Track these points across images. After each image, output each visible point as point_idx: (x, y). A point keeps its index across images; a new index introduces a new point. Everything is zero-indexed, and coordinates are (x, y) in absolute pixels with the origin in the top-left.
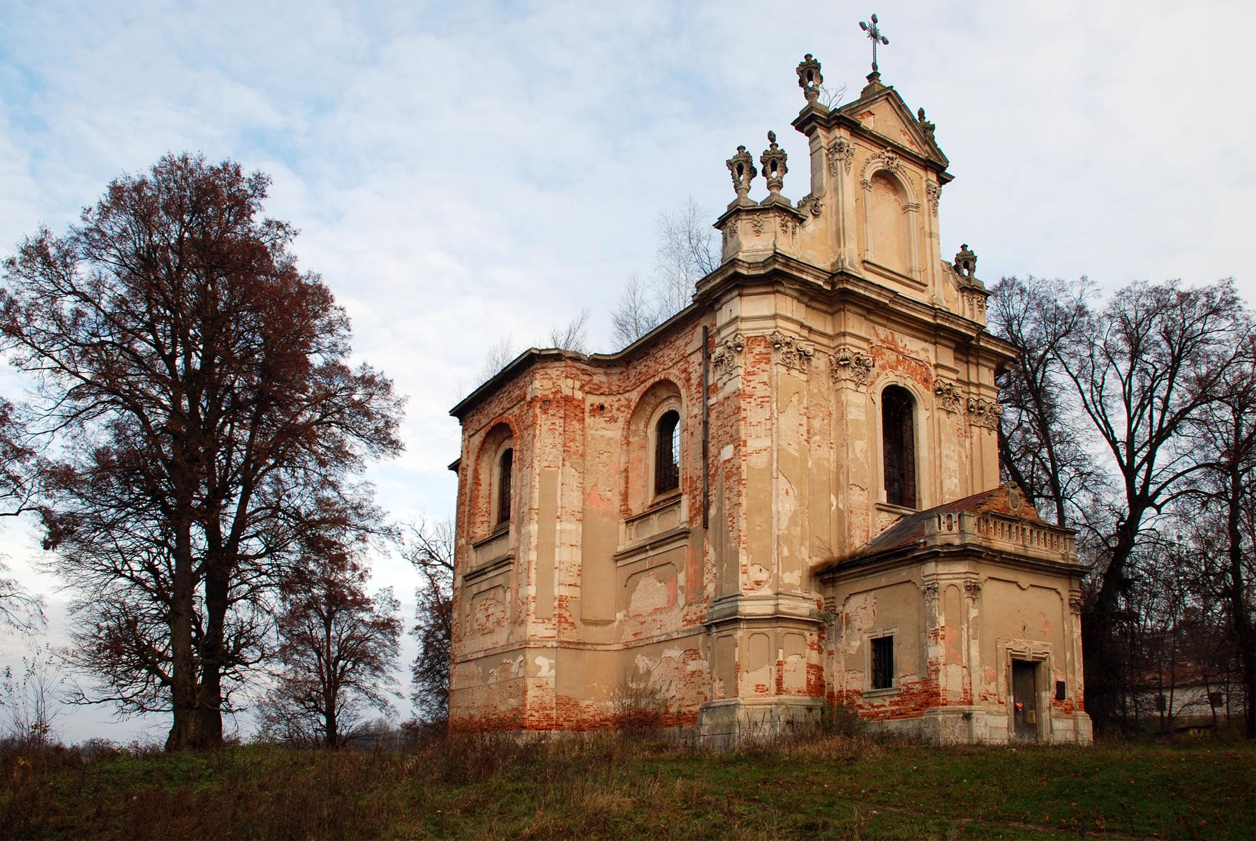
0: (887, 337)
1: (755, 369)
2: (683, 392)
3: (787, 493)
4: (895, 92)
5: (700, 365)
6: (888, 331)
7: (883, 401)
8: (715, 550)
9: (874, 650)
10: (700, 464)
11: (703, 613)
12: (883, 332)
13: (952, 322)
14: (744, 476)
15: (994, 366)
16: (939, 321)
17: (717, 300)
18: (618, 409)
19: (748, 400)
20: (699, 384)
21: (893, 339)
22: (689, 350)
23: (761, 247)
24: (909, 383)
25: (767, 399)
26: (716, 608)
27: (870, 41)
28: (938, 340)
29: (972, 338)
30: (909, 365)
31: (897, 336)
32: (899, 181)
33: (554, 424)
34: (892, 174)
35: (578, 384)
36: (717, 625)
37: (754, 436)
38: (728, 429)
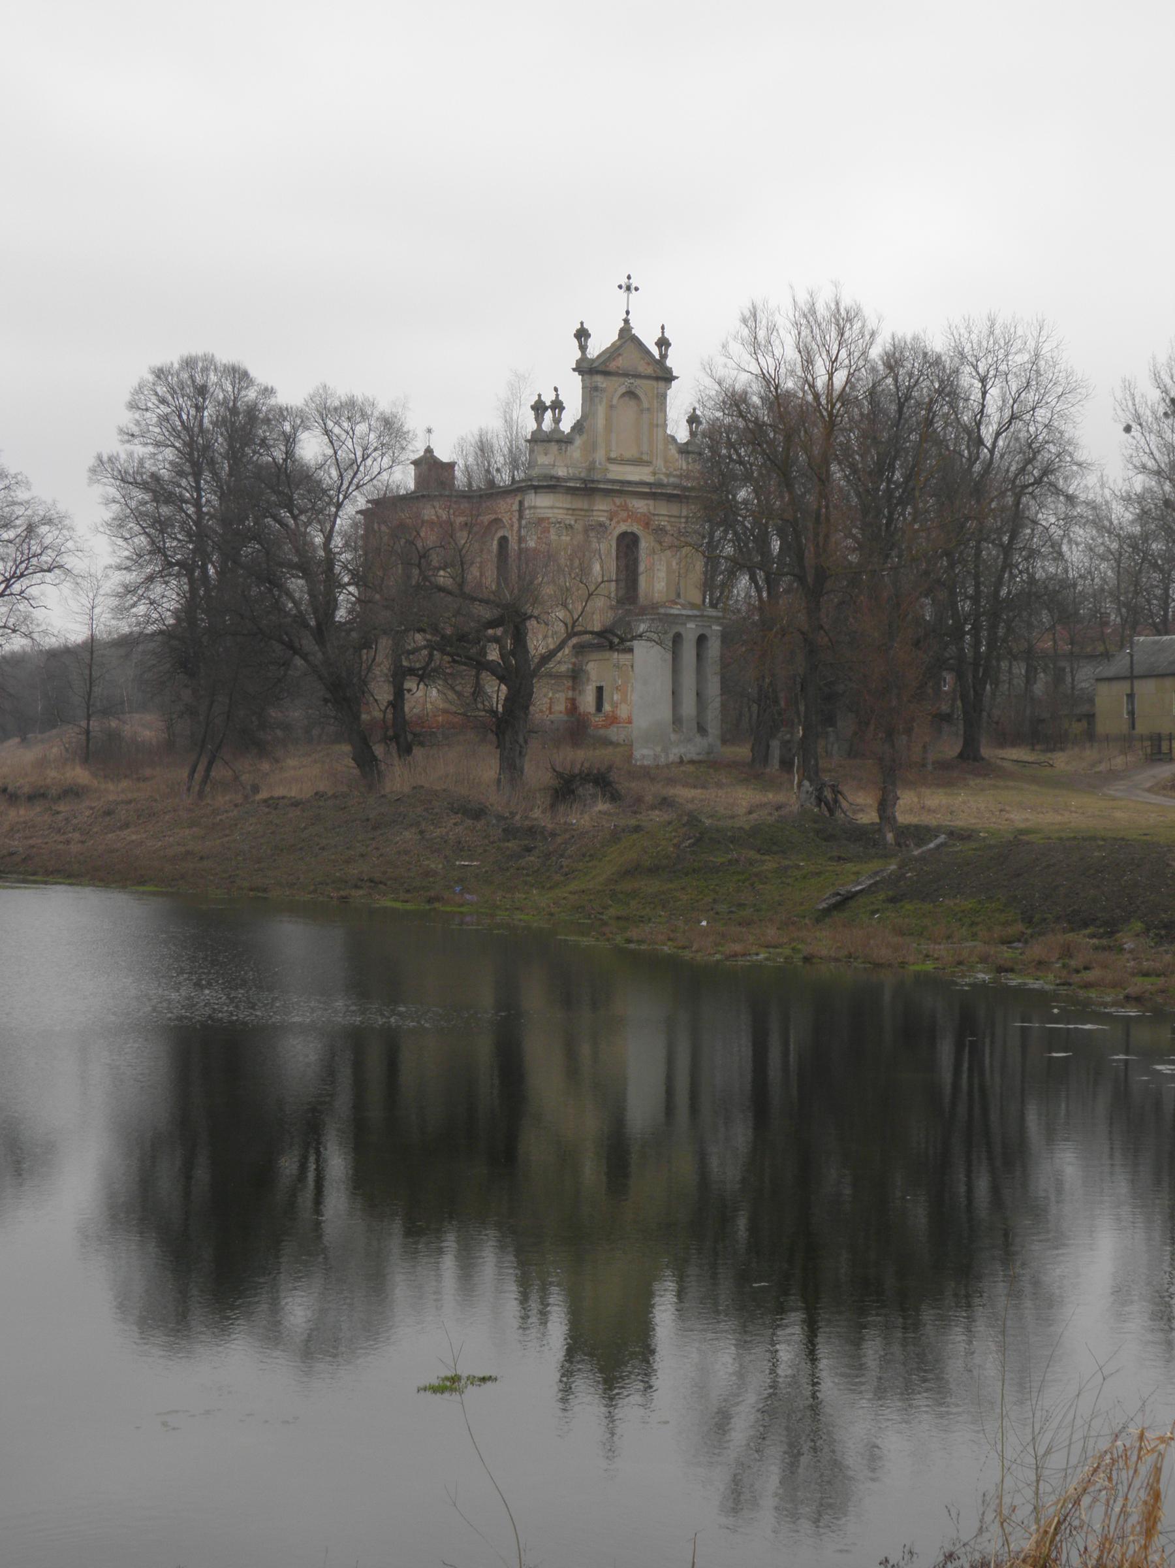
12: (618, 501)
24: (636, 528)
31: (628, 501)
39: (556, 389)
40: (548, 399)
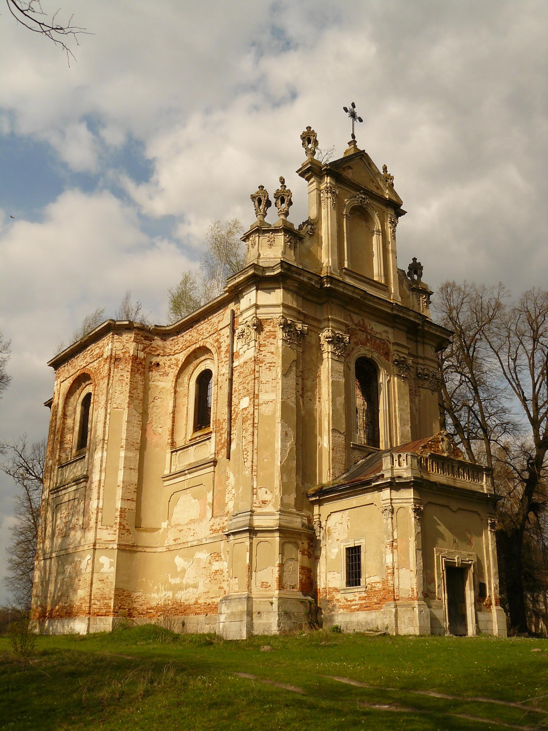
0: (359, 322)
1: (265, 342)
2: (215, 356)
3: (286, 434)
4: (366, 154)
5: (228, 337)
6: (360, 318)
7: (356, 368)
8: (234, 475)
9: (348, 557)
10: (226, 410)
11: (224, 525)
12: (356, 318)
13: (404, 313)
14: (256, 421)
15: (435, 344)
16: (395, 312)
17: (241, 292)
18: (169, 366)
19: (260, 365)
20: (227, 351)
21: (364, 323)
22: (221, 325)
23: (272, 256)
25: (274, 365)
26: (234, 521)
27: (351, 119)
28: (395, 325)
29: (419, 324)
30: (375, 342)
31: (366, 321)
32: (368, 212)
33: (122, 376)
34: (364, 209)
35: (141, 347)
36: (234, 534)
37: (264, 391)
38: (245, 385)
39: (282, 181)
40: (273, 187)
